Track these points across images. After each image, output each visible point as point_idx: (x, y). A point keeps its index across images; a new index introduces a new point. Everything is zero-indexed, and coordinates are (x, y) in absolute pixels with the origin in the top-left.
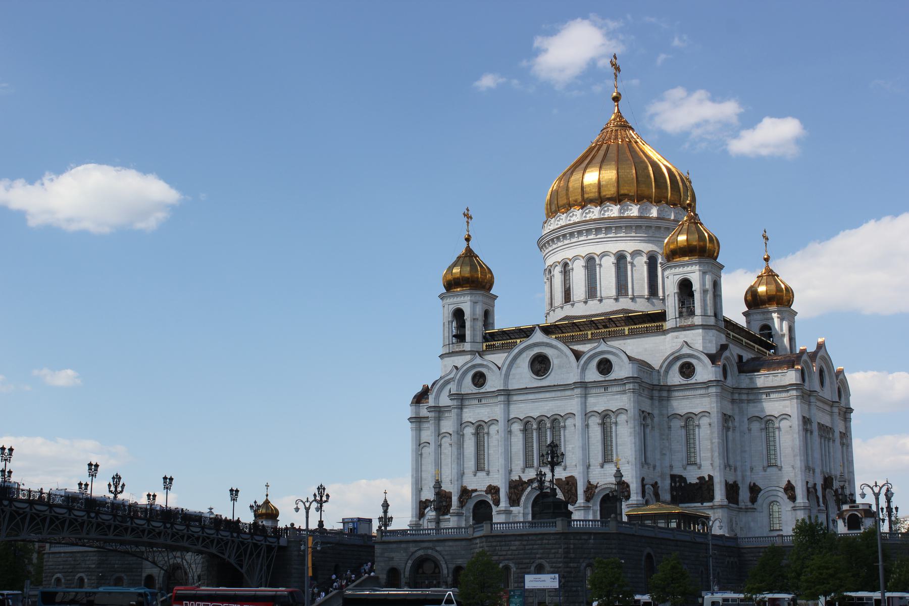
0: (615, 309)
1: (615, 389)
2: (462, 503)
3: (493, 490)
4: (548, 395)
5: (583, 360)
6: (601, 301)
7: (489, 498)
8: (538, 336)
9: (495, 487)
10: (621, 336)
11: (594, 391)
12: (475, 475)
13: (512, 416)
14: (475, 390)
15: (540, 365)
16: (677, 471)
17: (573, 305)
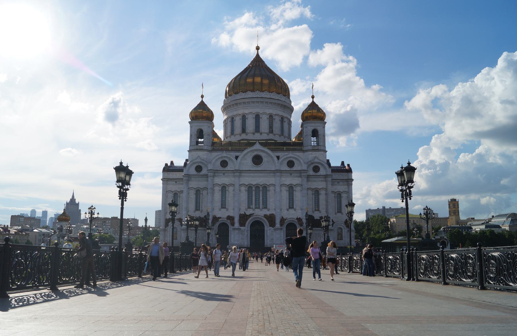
1: (295, 175)
2: (213, 223)
3: (231, 218)
4: (261, 175)
5: (281, 160)
6: (261, 134)
7: (228, 222)
8: (257, 146)
9: (231, 217)
10: (282, 150)
11: (285, 175)
12: (220, 210)
13: (241, 183)
14: (222, 169)
15: (257, 160)
16: (310, 213)
17: (247, 134)
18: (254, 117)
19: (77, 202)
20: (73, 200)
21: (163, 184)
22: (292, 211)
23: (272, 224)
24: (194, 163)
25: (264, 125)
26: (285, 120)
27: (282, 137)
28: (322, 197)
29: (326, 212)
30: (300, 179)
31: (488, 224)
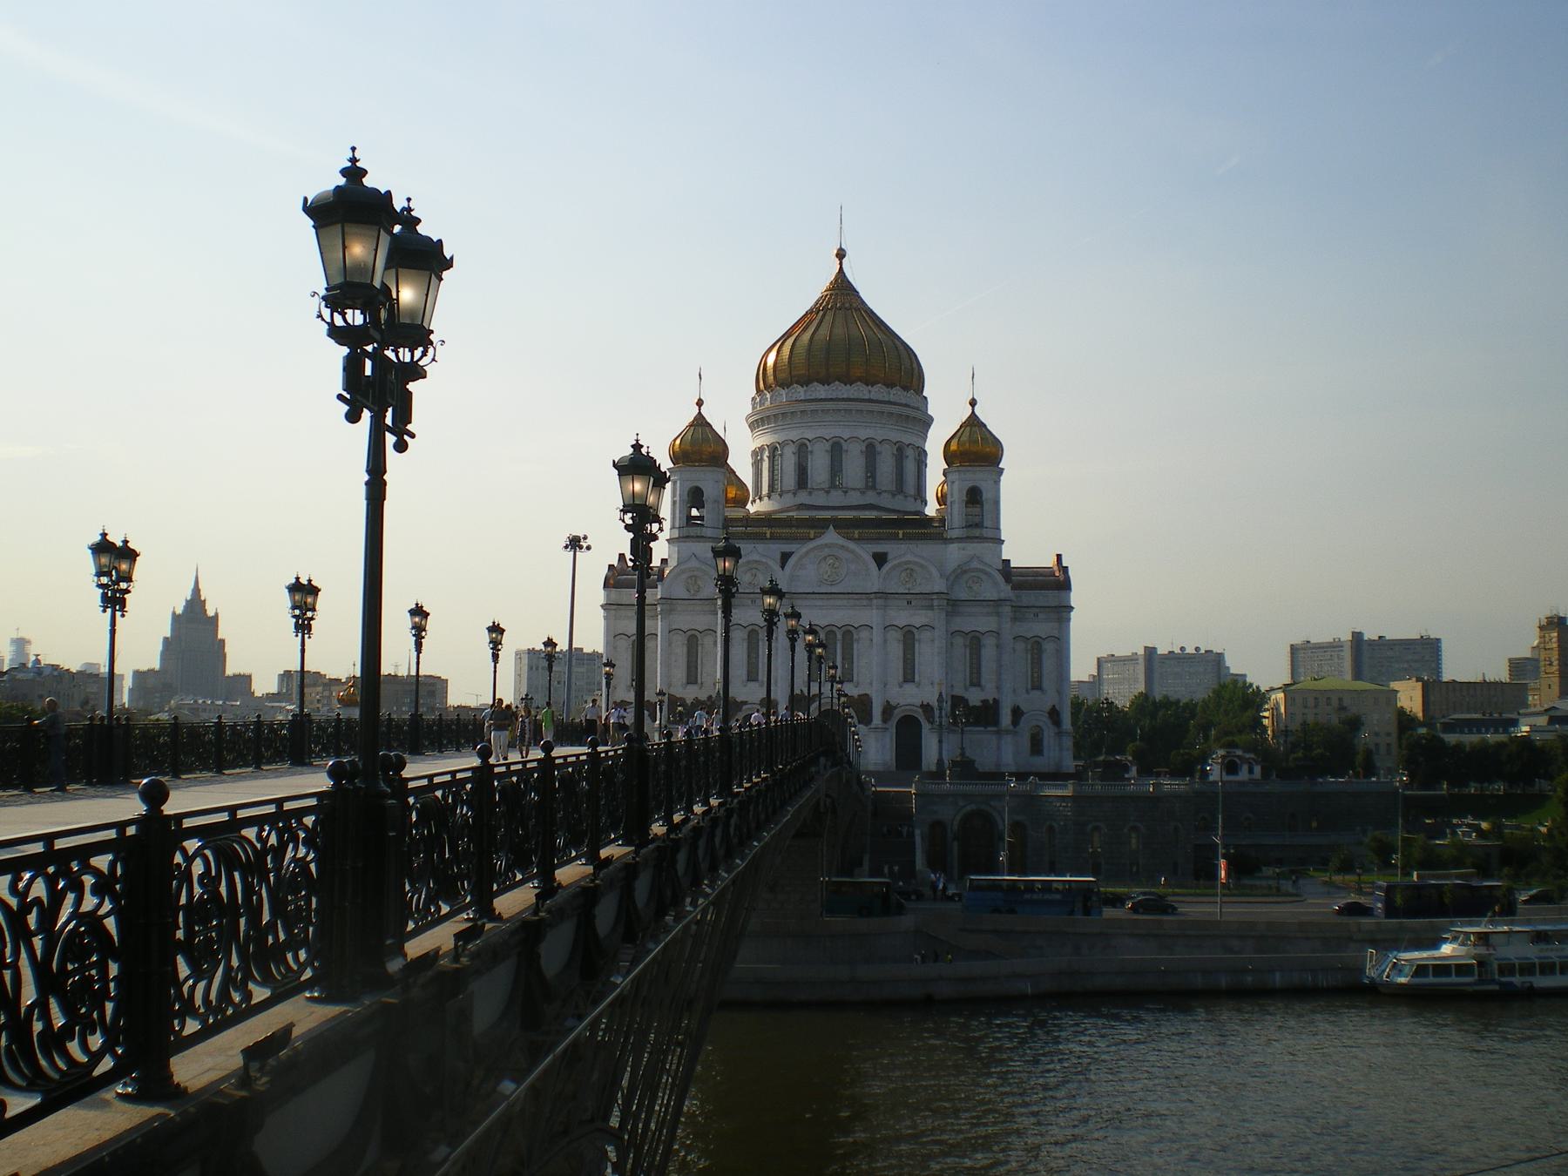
0: (862, 503)
4: (839, 603)
5: (886, 567)
8: (831, 536)
10: (895, 537)
16: (958, 692)
18: (828, 446)
19: (211, 613)
20: (196, 603)
21: (606, 618)
22: (909, 688)
23: (866, 718)
24: (683, 572)
25: (854, 469)
26: (909, 452)
27: (900, 497)
28: (988, 652)
29: (998, 688)
30: (930, 613)
31: (1553, 713)
